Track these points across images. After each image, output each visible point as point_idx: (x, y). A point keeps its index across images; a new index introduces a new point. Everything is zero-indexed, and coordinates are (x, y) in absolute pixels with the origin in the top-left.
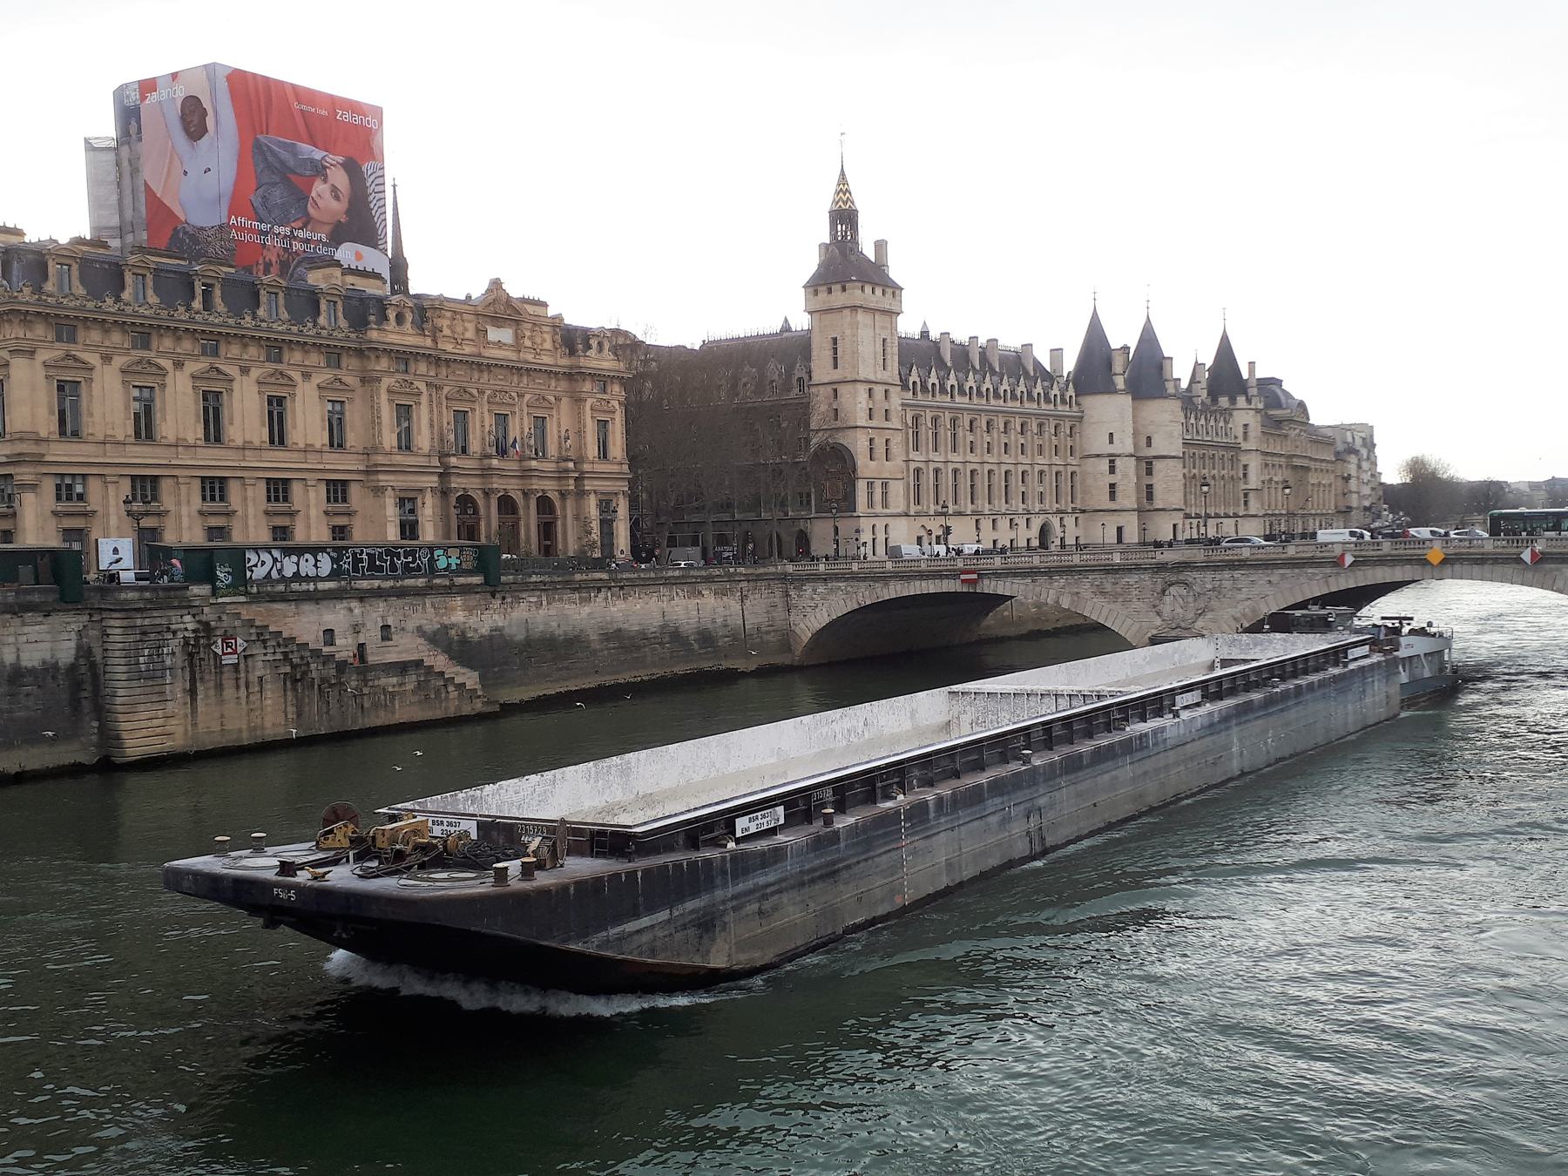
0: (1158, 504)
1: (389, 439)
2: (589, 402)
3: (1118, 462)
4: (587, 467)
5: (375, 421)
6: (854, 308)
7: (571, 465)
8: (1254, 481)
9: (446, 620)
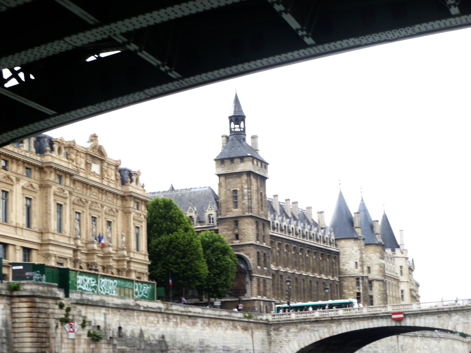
1: (53, 225)
2: (133, 214)
3: (361, 281)
4: (132, 255)
5: (46, 213)
6: (249, 173)
7: (125, 253)
9: (144, 328)
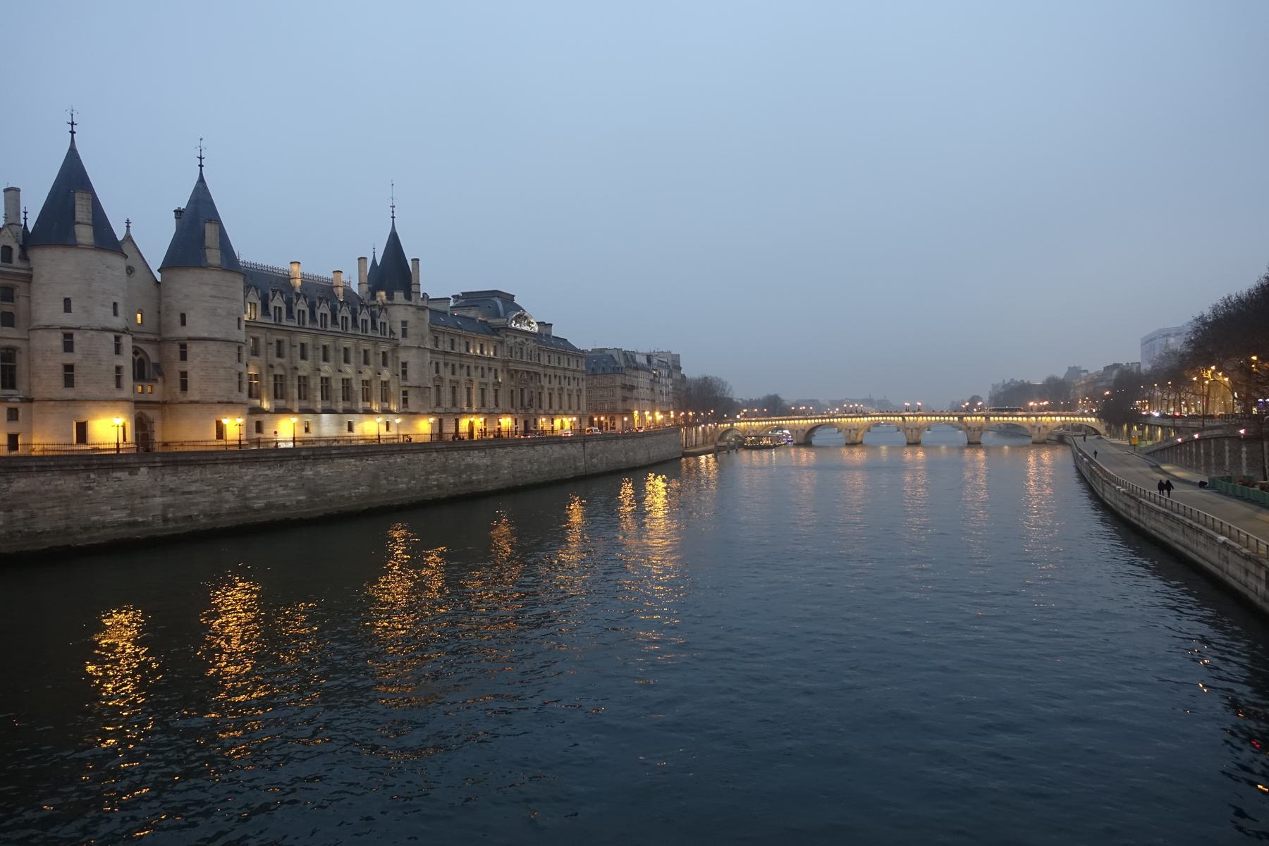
3: (77, 337)
8: (413, 377)
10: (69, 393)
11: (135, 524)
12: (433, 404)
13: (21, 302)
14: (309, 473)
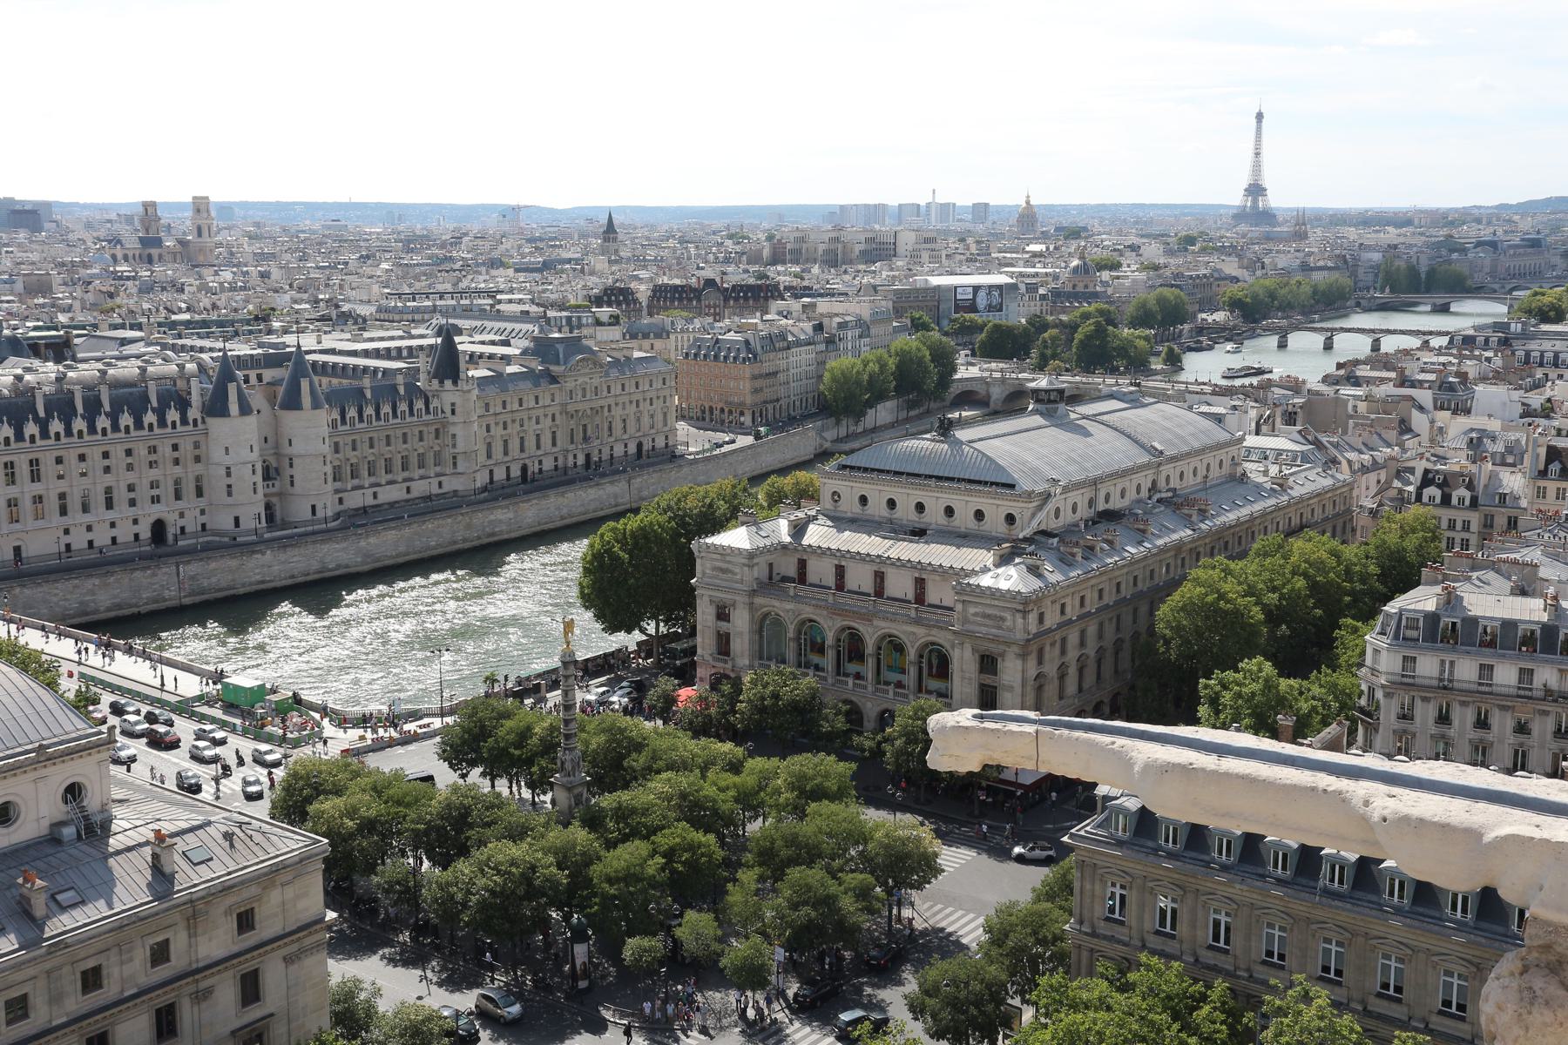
0: (298, 489)
8: (460, 447)
10: (230, 500)
11: (263, 582)
12: (482, 458)
13: (203, 447)
14: (363, 543)
